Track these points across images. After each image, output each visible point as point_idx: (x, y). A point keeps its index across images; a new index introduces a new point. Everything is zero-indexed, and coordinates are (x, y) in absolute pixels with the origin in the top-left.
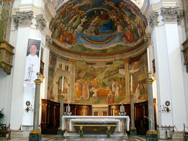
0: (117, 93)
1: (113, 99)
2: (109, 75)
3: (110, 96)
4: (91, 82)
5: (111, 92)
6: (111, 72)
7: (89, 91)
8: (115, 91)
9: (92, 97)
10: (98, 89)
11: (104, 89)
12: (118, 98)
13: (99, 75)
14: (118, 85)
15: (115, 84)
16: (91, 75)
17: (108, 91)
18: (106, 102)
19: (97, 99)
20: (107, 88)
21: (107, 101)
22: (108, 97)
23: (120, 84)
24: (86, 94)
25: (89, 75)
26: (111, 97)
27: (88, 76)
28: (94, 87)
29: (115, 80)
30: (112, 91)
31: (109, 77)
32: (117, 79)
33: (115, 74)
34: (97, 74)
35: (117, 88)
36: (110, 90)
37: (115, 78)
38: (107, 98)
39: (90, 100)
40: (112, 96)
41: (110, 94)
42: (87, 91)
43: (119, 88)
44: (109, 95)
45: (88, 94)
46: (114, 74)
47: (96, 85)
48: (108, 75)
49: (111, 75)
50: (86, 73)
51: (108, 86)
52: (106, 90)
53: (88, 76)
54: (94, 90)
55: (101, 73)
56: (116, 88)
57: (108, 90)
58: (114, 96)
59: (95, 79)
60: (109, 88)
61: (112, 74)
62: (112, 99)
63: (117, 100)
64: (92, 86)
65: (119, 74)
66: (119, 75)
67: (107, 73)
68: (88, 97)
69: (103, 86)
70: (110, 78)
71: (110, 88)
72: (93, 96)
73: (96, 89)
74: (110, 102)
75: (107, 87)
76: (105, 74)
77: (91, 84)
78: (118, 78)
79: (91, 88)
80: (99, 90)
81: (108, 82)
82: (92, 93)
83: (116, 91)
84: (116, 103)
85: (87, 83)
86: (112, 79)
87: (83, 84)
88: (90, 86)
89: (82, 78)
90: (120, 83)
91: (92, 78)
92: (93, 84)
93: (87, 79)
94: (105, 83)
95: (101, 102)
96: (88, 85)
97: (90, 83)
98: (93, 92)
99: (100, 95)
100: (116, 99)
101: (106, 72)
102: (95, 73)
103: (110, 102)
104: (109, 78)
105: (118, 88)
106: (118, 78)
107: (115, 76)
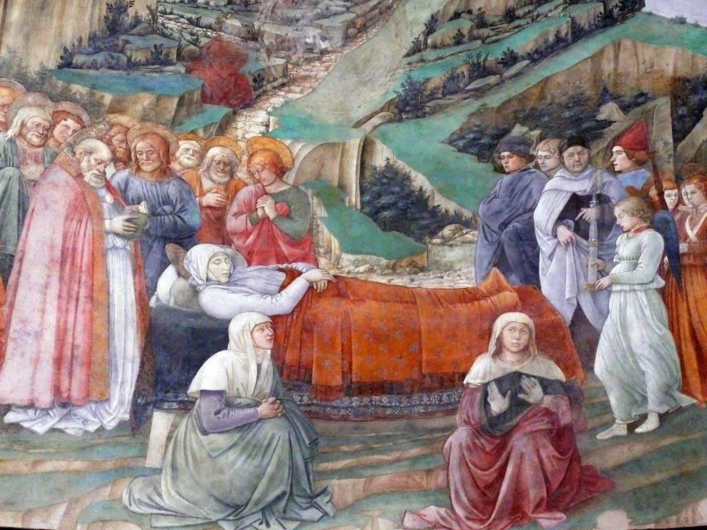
0: (624, 326)
1: (561, 437)
2: (480, 70)
3: (511, 383)
4: (185, 152)
5: (519, 318)
6: (510, 16)
7: (145, 293)
8: (597, 292)
9: (186, 406)
10: (293, 275)
11: (397, 281)
12: (654, 406)
13: (318, 69)
14: (631, 203)
15: (582, 187)
16: (193, 60)
17: (462, 309)
18: (442, 494)
19: (275, 432)
20: (452, 255)
21: (455, 476)
22: (469, 409)
23: (679, 181)
24: (81, 339)
25: (158, 60)
26: (518, 405)
27: (132, 65)
28: (223, 238)
29: (576, 121)
30: (530, 298)
31: (480, 93)
32: (609, 110)
33: (579, 34)
34: (282, 45)
35: (624, 246)
36: (500, 289)
37: (578, 100)
38: (451, 429)
39: (144, 456)
40: (546, 385)
41: (509, 357)
42: (99, 298)
43: (671, 250)
44: (481, 370)
45: (109, 339)
46: (559, 45)
47: (267, 208)
48: (459, 61)
49: (511, 59)
50: (114, 26)
51: (467, 224)
52: (437, 299)
53: (132, 65)
54: (231, 281)
55: (347, 39)
56: (606, 255)
57: (468, 296)
58: (570, 393)
59: (251, 124)
60: (486, 254)
61: (524, 41)
62: (548, 452)
63: (638, 449)
64: (194, 218)
65: (656, 29)
66: (649, 40)
67: (445, 32)
68: (104, 399)
69: (386, 226)
70: (494, 100)
71: (500, 261)
72: (194, 387)
73: (260, 276)
74: (518, 492)
75: (446, 242)
76: (417, 49)
77: (172, 189)
78: (642, 98)
79: (177, 262)
80: (311, 290)
81: (469, 162)
82: (194, 331)
83: (614, 302)
84: (617, 503)
85: (119, 176)
86: (531, 118)
87: (32, 171)
88: (153, 213)
89: (30, 87)
90: (668, 167)
91: (205, 99)
92: (211, 199)
93: (108, 98)
94: (420, 181)
95: (344, 488)
96: (123, 197)
97: (164, 171)
98: (202, 314)
99: (337, 381)
100: (620, 429)
101: (431, 28)
102: (254, 36)
103: (518, 492)
104: (475, 105)
105: (651, 241)
106: (628, 96)
107: (588, 67)
